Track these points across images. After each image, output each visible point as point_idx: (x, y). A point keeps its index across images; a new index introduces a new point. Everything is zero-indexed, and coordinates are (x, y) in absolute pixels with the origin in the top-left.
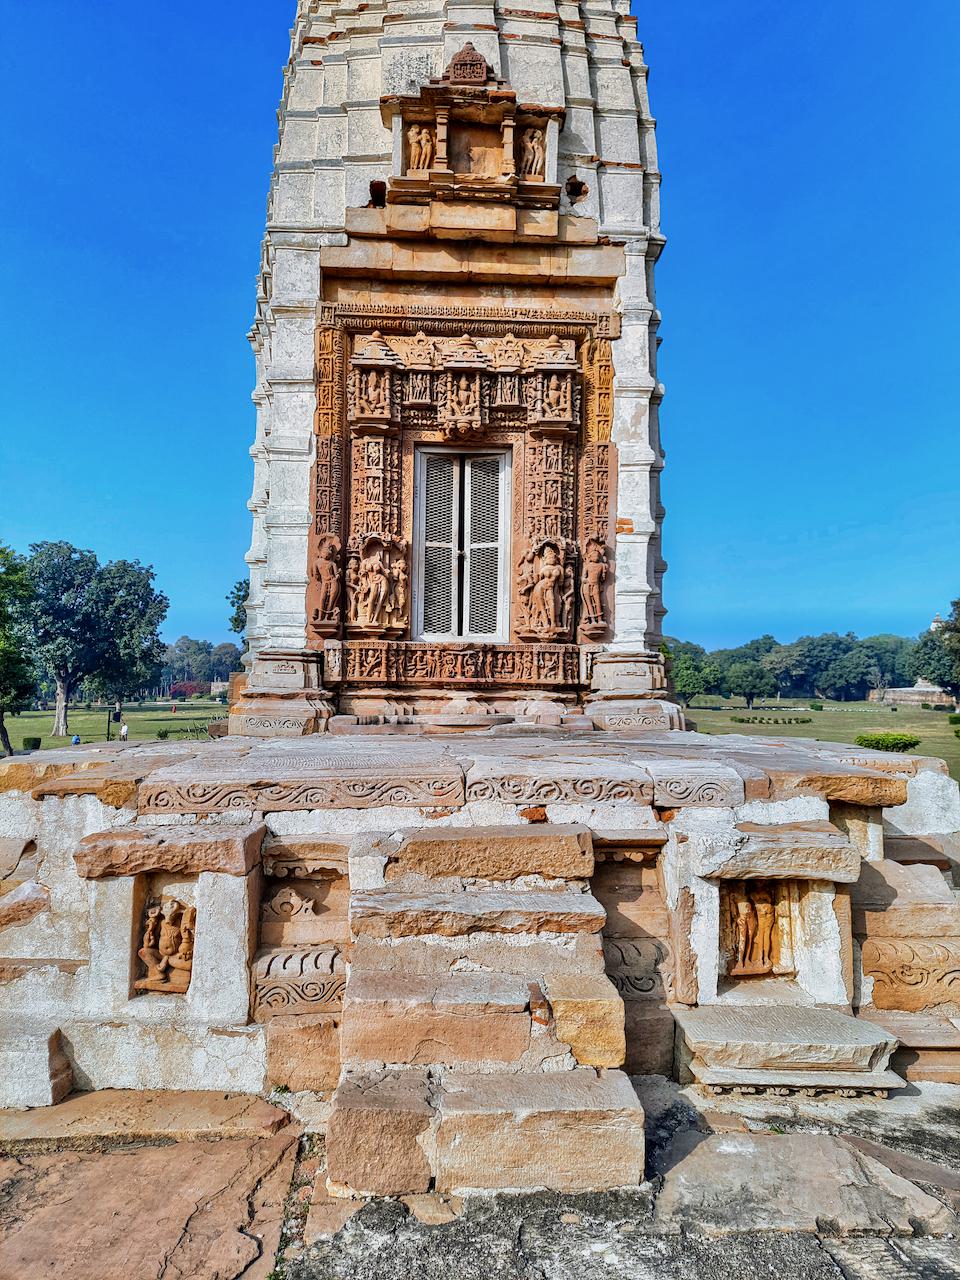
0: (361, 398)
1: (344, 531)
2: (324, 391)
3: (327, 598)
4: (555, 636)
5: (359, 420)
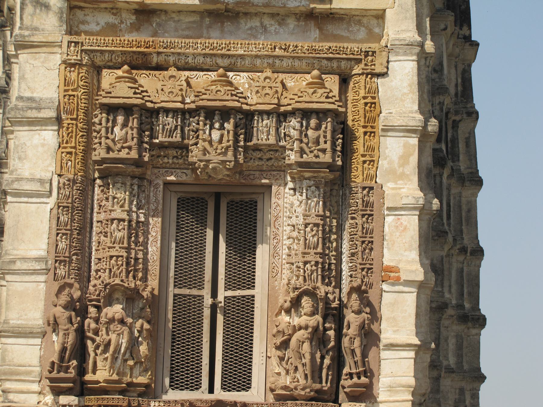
0: (107, 138)
1: (84, 277)
2: (68, 128)
3: (63, 350)
4: (312, 393)
5: (103, 161)
